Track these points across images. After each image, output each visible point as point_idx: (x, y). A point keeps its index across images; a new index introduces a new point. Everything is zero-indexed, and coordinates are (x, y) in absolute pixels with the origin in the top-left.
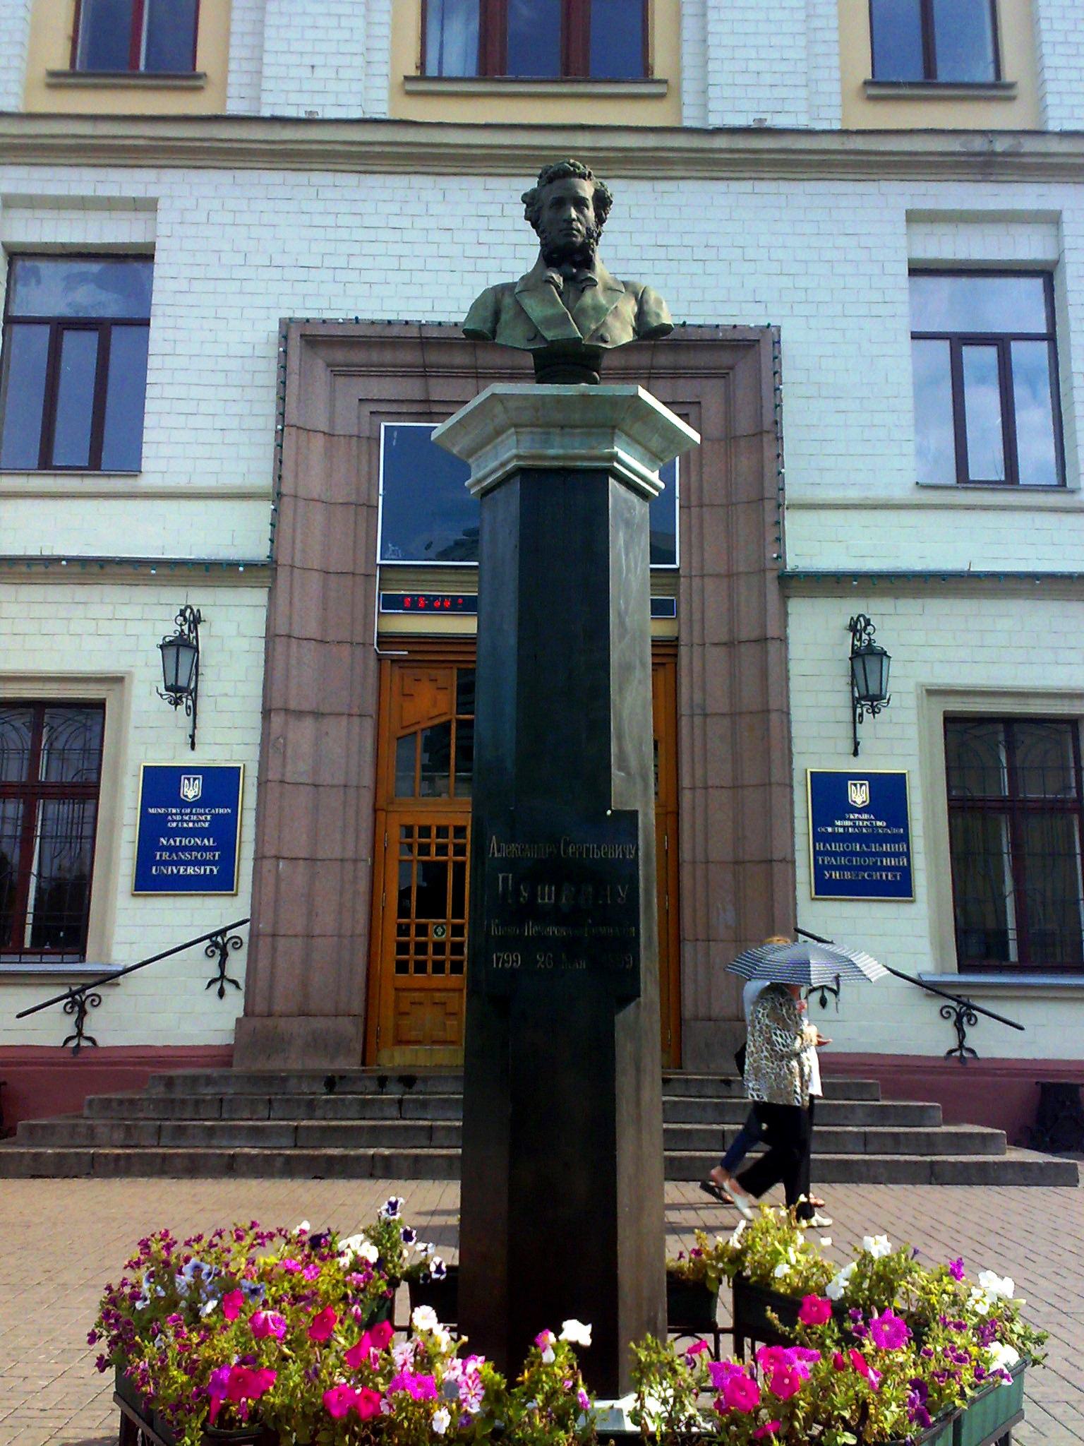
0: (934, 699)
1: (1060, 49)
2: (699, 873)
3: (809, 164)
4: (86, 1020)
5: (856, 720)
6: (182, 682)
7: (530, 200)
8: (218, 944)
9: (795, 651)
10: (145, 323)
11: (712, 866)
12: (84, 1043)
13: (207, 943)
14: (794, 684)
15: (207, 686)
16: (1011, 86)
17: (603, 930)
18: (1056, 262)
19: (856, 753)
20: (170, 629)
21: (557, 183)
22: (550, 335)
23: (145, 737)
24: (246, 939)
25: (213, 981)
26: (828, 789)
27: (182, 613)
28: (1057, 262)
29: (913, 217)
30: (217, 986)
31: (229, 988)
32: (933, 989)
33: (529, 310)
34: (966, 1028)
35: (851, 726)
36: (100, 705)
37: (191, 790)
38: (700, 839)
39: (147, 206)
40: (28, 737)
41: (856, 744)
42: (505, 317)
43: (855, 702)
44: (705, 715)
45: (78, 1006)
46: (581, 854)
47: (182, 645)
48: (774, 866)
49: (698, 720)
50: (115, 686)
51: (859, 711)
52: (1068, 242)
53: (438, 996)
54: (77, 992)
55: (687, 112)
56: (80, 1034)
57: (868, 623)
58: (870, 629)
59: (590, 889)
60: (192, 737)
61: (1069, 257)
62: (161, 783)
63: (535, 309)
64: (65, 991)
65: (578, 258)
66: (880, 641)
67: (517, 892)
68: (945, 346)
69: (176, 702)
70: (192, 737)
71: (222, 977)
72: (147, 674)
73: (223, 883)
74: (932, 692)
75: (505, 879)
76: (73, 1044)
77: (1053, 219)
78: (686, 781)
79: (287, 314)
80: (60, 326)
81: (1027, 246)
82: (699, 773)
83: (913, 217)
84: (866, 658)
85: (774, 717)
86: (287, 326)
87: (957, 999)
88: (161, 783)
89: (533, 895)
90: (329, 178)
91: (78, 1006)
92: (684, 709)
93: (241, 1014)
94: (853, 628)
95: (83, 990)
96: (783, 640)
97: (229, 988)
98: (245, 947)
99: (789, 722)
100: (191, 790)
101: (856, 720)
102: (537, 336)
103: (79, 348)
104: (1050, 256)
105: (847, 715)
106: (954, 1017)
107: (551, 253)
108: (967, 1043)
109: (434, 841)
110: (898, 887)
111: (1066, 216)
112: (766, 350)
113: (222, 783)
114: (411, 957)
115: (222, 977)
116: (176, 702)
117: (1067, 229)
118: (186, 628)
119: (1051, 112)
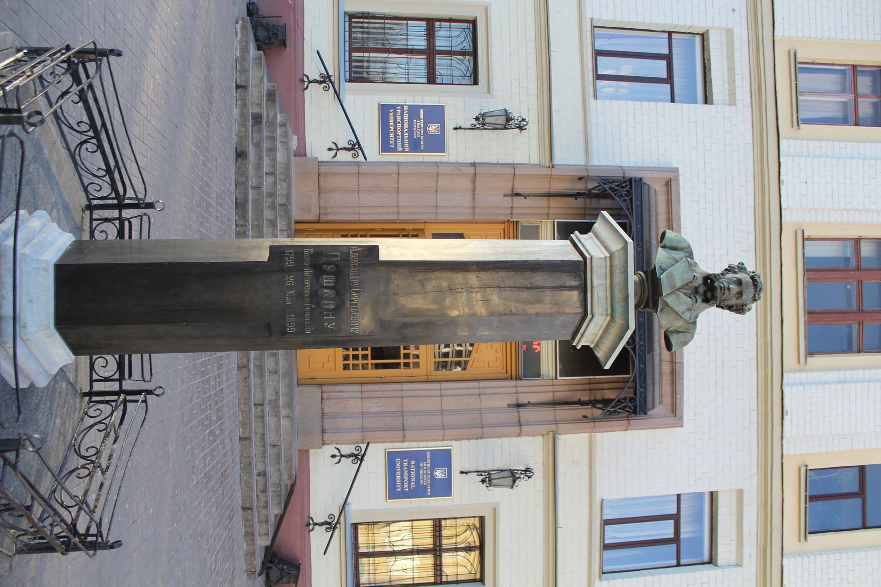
4: (317, 85)
6: (488, 120)
7: (741, 268)
8: (355, 146)
9: (514, 440)
10: (673, 101)
12: (306, 84)
13: (355, 141)
15: (488, 135)
17: (307, 315)
18: (716, 565)
19: (462, 472)
20: (515, 114)
22: (663, 277)
23: (458, 104)
24: (357, 160)
25: (336, 145)
26: (444, 458)
27: (523, 120)
28: (716, 565)
29: (740, 493)
30: (334, 147)
31: (333, 153)
36: (476, 83)
37: (433, 129)
38: (414, 393)
39: (732, 102)
40: (458, 49)
41: (466, 473)
45: (326, 79)
46: (353, 301)
47: (507, 122)
48: (403, 431)
49: (477, 391)
52: (727, 571)
54: (330, 80)
56: (310, 82)
57: (529, 477)
58: (526, 478)
59: (332, 307)
60: (460, 128)
62: (436, 114)
64: (331, 73)
67: (329, 264)
68: (675, 511)
69: (477, 119)
70: (460, 128)
71: (338, 149)
72: (493, 105)
73: (385, 146)
75: (337, 256)
76: (306, 79)
78: (444, 385)
79: (681, 172)
80: (668, 58)
81: (725, 553)
82: (451, 392)
84: (513, 476)
85: (479, 431)
86: (675, 171)
88: (436, 114)
89: (327, 273)
90: (751, 191)
91: (326, 79)
92: (483, 384)
93: (320, 159)
95: (331, 82)
96: (520, 435)
97: (333, 153)
98: (353, 160)
99: (477, 439)
100: (433, 129)
103: (659, 69)
104: (719, 562)
106: (329, 521)
107: (711, 280)
108: (316, 527)
110: (393, 493)
111: (740, 569)
112: (672, 420)
113: (437, 144)
115: (338, 149)
116: (477, 119)
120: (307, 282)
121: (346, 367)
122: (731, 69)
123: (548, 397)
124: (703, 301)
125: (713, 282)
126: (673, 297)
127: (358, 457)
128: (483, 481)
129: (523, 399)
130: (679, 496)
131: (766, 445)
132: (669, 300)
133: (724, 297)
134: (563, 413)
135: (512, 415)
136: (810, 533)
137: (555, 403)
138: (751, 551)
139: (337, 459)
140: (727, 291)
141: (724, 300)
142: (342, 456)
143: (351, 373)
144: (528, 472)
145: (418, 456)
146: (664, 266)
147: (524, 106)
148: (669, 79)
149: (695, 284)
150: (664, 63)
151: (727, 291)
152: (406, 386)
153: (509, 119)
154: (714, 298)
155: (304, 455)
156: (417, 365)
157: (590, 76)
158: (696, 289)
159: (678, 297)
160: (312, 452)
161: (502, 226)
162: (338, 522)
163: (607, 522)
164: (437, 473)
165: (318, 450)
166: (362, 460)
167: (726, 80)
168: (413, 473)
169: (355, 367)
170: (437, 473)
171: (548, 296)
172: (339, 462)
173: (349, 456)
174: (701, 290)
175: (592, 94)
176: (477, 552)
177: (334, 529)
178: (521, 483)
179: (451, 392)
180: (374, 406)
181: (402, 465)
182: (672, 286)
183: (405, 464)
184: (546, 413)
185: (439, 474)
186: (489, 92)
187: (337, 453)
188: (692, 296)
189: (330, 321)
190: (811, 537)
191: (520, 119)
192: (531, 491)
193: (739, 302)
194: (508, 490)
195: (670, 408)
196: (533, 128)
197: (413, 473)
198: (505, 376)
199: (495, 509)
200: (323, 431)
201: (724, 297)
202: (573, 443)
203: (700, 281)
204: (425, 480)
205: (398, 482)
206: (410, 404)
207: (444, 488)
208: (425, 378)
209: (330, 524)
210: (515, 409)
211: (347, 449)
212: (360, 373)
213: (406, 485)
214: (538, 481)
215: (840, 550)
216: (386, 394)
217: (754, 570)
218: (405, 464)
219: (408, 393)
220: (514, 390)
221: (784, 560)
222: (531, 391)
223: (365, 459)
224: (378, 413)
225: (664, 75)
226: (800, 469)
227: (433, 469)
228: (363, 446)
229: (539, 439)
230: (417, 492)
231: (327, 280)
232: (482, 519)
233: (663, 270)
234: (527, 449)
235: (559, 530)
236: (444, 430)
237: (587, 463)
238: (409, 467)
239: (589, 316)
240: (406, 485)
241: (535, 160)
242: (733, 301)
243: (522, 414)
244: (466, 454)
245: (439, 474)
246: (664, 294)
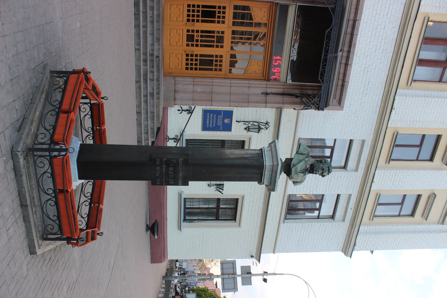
0: (249, 139)
1: (394, 174)
2: (209, 83)
9: (263, 109)
11: (211, 87)
16: (389, 162)
18: (346, 170)
19: (237, 121)
21: (327, 169)
26: (229, 114)
28: (346, 170)
29: (363, 141)
32: (182, 135)
34: (173, 140)
38: (218, 84)
41: (239, 122)
44: (249, 87)
48: (211, 101)
49: (248, 85)
52: (350, 173)
53: (182, 15)
55: (402, 91)
57: (267, 129)
61: (347, 173)
66: (262, 131)
67: (171, 164)
68: (332, 145)
77: (356, 170)
78: (233, 81)
81: (352, 164)
82: (236, 85)
85: (247, 104)
87: (180, 139)
89: (171, 166)
94: (267, 123)
96: (266, 107)
109: (221, 15)
110: (205, 128)
111: (356, 173)
114: (191, 18)
117: (353, 173)
119: (380, 171)
120: (164, 169)
121: (187, 69)
123: (280, 91)
125: (314, 167)
127: (190, 112)
128: (245, 129)
129: (269, 91)
131: (380, 122)
134: (286, 99)
135: (263, 98)
137: (283, 94)
139: (180, 112)
142: (183, 110)
143: (189, 71)
145: (218, 113)
152: (215, 80)
155: (165, 110)
156: (220, 70)
160: (169, 108)
161: (270, 4)
162: (180, 139)
164: (226, 121)
165: (172, 108)
166: (192, 113)
168: (215, 120)
169: (191, 69)
170: (226, 121)
172: (181, 113)
173: (186, 111)
177: (178, 141)
179: (236, 85)
180: (199, 89)
181: (210, 116)
183: (211, 116)
184: (279, 98)
185: (226, 121)
187: (180, 109)
189: (171, 181)
195: (338, 101)
197: (215, 120)
198: (262, 78)
199: (250, 138)
200: (175, 100)
202: (289, 113)
203: (308, 166)
204: (220, 123)
205: (208, 123)
206: (215, 89)
207: (228, 128)
208: (224, 76)
209: (176, 139)
210: (264, 95)
211: (185, 107)
212: (194, 72)
213: (211, 125)
216: (205, 83)
217: (362, 173)
218: (211, 116)
219: (215, 84)
220: (265, 86)
221: (377, 171)
222: (273, 88)
223: (194, 112)
224: (200, 92)
226: (394, 133)
227: (224, 119)
228: (193, 107)
230: (216, 128)
231: (171, 169)
233: (294, 166)
234: (267, 114)
236: (230, 102)
238: (213, 117)
240: (211, 125)
243: (267, 98)
244: (241, 113)
245: (226, 121)
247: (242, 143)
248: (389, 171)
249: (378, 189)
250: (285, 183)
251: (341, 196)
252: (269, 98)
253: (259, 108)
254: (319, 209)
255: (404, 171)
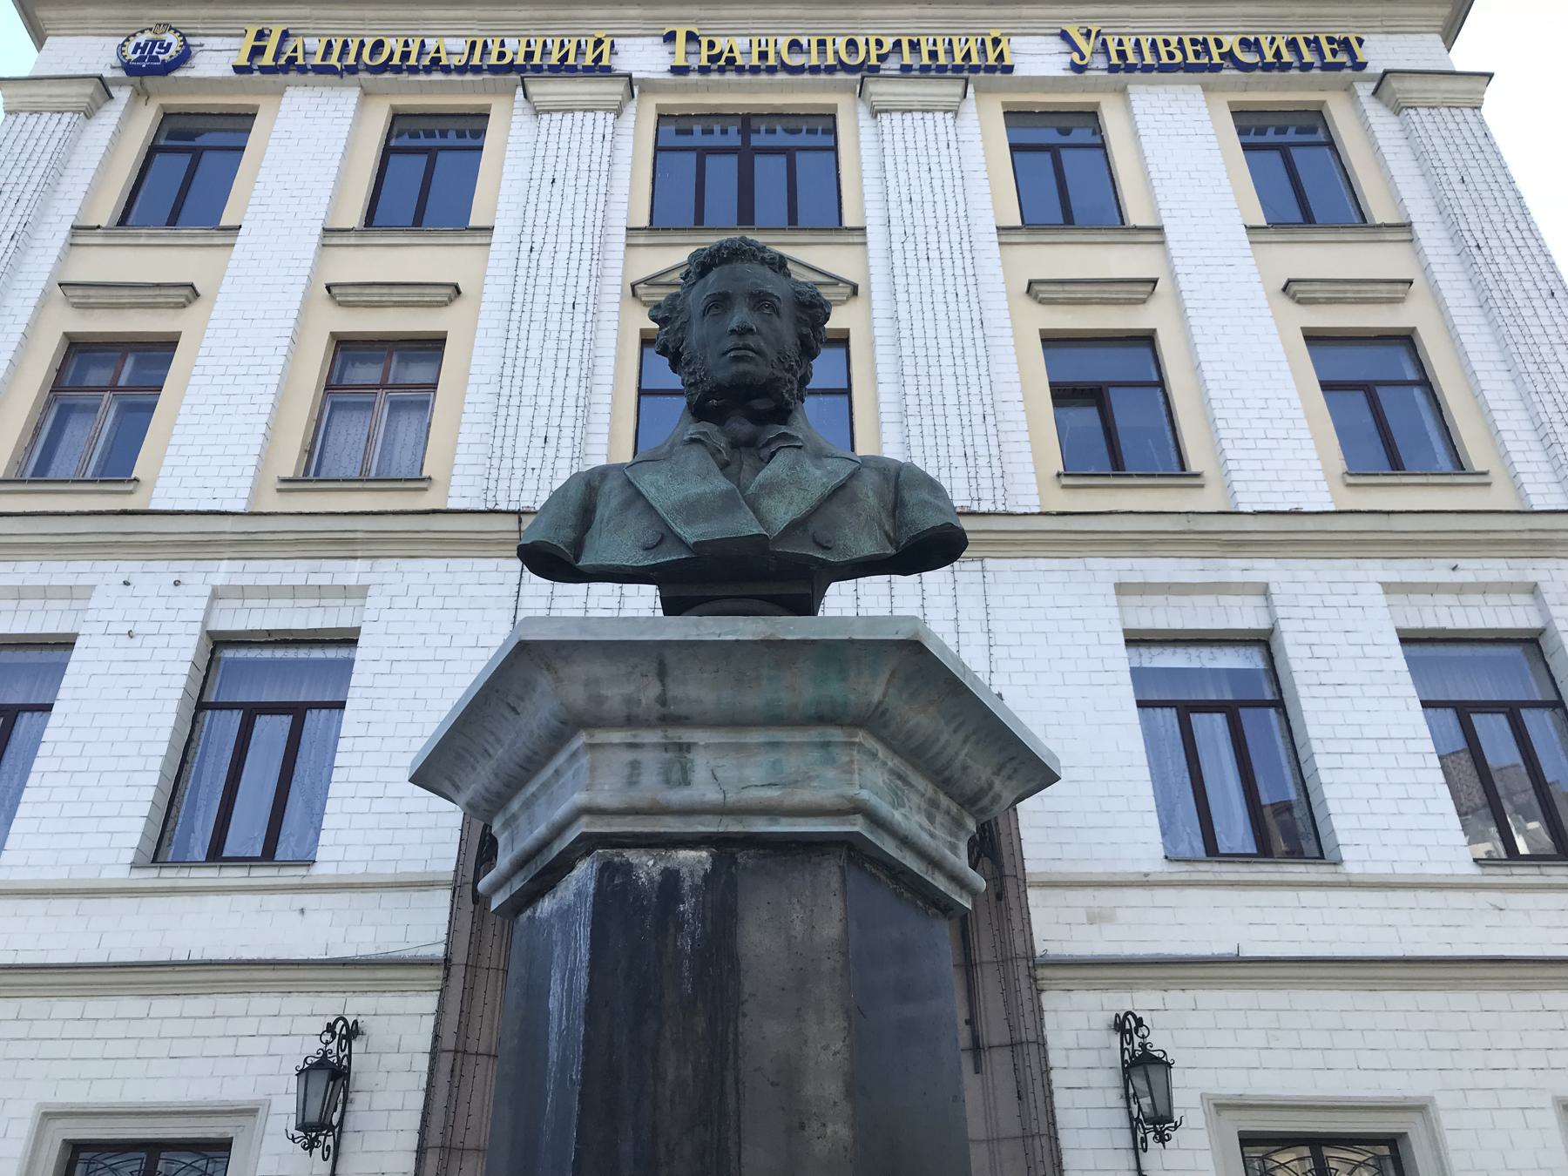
0: (1225, 1114)
3: (1013, 543)
5: (1138, 1147)
10: (341, 706)
14: (1061, 1099)
16: (1197, 475)
18: (1271, 631)
21: (712, 276)
22: (690, 534)
27: (330, 1028)
28: (1271, 631)
29: (1121, 589)
33: (649, 492)
35: (1131, 1154)
39: (360, 592)
42: (603, 511)
43: (1134, 1124)
50: (242, 1120)
51: (1140, 1135)
52: (1280, 612)
57: (1139, 1022)
61: (1283, 625)
63: (660, 488)
65: (760, 404)
69: (310, 1146)
74: (1222, 1106)
80: (252, 712)
83: (1121, 589)
96: (1042, 1044)
99: (1059, 1151)
101: (1138, 1147)
102: (667, 536)
103: (271, 730)
104: (1263, 624)
105: (1125, 1139)
107: (707, 396)
111: (1273, 589)
116: (310, 1146)
118: (333, 1046)
119: (1239, 497)
122: (294, 592)
124: (784, 422)
125: (719, 390)
126: (767, 504)
128: (1162, 1138)
130: (1141, 704)
132: (782, 512)
133: (772, 355)
135: (999, 1062)
136: (1183, 469)
138: (1234, 569)
140: (751, 341)
141: (782, 358)
144: (1125, 1026)
146: (650, 537)
147: (294, 1027)
148: (297, 712)
149: (722, 442)
150: (262, 722)
151: (751, 341)
153: (322, 1063)
154: (768, 388)
157: (263, 875)
158: (735, 444)
159: (771, 488)
163: (1212, 850)
167: (316, 602)
171: (764, 1033)
174: (743, 428)
175: (302, 871)
176: (1327, 1152)
178: (1158, 1041)
182: (728, 504)
184: (988, 982)
186: (252, 1112)
188: (765, 453)
190: (1194, 465)
191: (327, 1037)
192: (1178, 1023)
193: (785, 308)
194: (1175, 1073)
196: (356, 1006)
201: (772, 355)
214: (1141, 1001)
215: (1210, 422)
217: (1270, 563)
225: (286, 721)
226: (1064, 487)
229: (1049, 1000)
232: (1248, 1140)
234: (1075, 1028)
235: (1247, 952)
237: (1089, 892)
239: (857, 826)
241: (430, 1002)
242: (786, 328)
243: (995, 1041)
246: (756, 530)
247: (1256, 1152)
248: (1231, 465)
249: (1324, 486)
250: (1421, 894)
251: (1404, 625)
252: (994, 1030)
253: (1055, 1076)
254: (1512, 711)
255: (1218, 414)
